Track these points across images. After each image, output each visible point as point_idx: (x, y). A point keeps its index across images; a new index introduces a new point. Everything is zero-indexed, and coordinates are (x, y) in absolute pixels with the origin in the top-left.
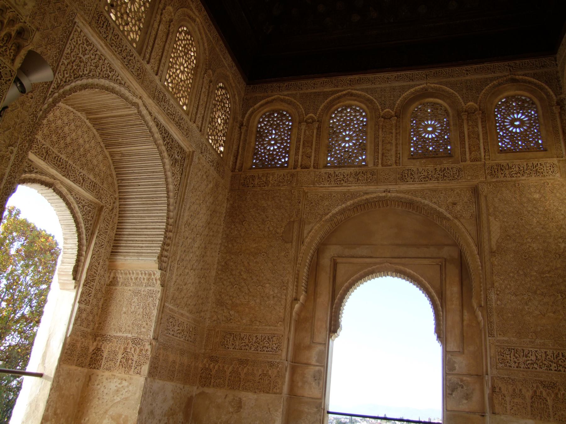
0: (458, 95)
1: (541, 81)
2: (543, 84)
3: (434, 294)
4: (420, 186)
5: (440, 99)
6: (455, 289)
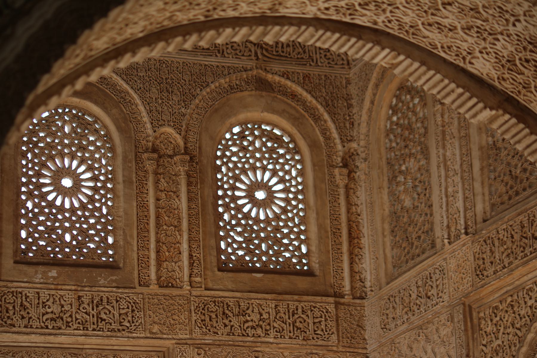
0: (138, 101)
1: (316, 99)
2: (319, 107)
4: (42, 338)
5: (96, 103)
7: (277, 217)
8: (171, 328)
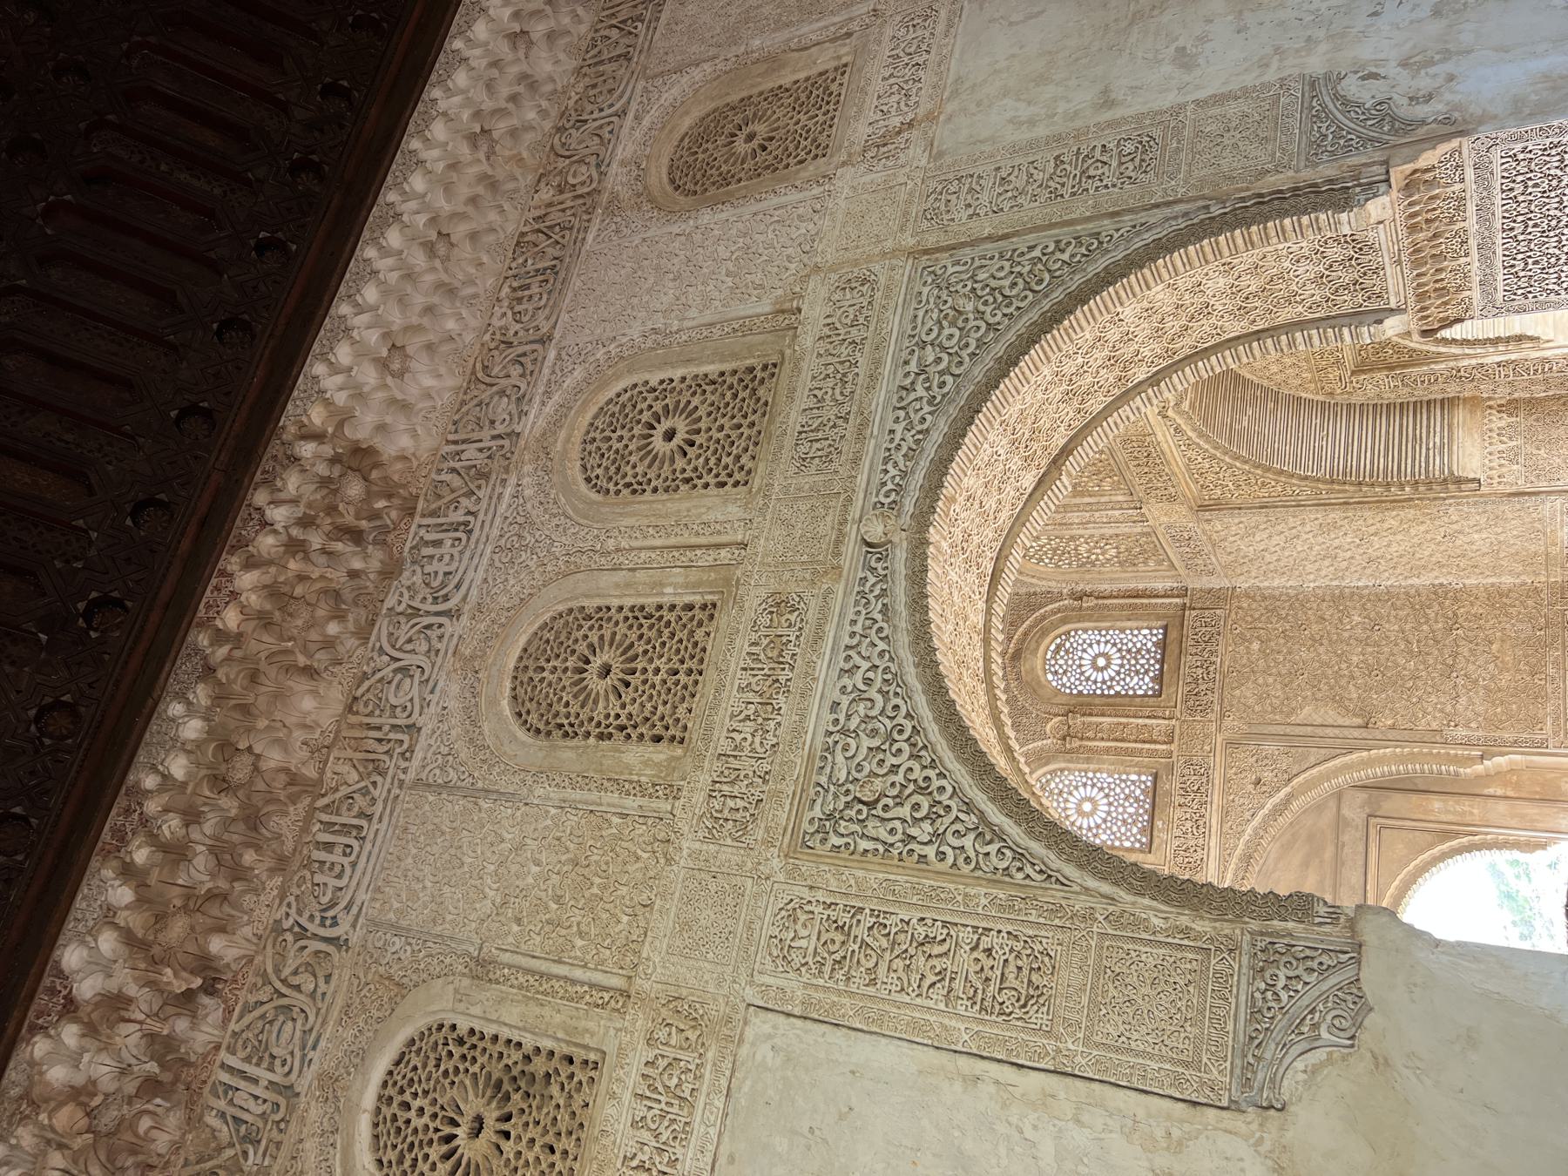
3: (1446, 846)
6: (1436, 804)
7: (1120, 650)
8: (1206, 736)
